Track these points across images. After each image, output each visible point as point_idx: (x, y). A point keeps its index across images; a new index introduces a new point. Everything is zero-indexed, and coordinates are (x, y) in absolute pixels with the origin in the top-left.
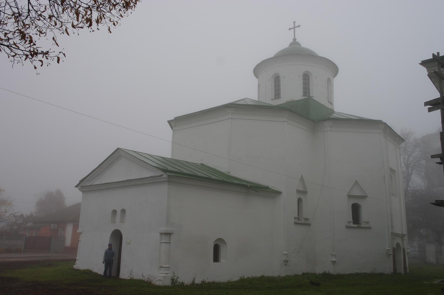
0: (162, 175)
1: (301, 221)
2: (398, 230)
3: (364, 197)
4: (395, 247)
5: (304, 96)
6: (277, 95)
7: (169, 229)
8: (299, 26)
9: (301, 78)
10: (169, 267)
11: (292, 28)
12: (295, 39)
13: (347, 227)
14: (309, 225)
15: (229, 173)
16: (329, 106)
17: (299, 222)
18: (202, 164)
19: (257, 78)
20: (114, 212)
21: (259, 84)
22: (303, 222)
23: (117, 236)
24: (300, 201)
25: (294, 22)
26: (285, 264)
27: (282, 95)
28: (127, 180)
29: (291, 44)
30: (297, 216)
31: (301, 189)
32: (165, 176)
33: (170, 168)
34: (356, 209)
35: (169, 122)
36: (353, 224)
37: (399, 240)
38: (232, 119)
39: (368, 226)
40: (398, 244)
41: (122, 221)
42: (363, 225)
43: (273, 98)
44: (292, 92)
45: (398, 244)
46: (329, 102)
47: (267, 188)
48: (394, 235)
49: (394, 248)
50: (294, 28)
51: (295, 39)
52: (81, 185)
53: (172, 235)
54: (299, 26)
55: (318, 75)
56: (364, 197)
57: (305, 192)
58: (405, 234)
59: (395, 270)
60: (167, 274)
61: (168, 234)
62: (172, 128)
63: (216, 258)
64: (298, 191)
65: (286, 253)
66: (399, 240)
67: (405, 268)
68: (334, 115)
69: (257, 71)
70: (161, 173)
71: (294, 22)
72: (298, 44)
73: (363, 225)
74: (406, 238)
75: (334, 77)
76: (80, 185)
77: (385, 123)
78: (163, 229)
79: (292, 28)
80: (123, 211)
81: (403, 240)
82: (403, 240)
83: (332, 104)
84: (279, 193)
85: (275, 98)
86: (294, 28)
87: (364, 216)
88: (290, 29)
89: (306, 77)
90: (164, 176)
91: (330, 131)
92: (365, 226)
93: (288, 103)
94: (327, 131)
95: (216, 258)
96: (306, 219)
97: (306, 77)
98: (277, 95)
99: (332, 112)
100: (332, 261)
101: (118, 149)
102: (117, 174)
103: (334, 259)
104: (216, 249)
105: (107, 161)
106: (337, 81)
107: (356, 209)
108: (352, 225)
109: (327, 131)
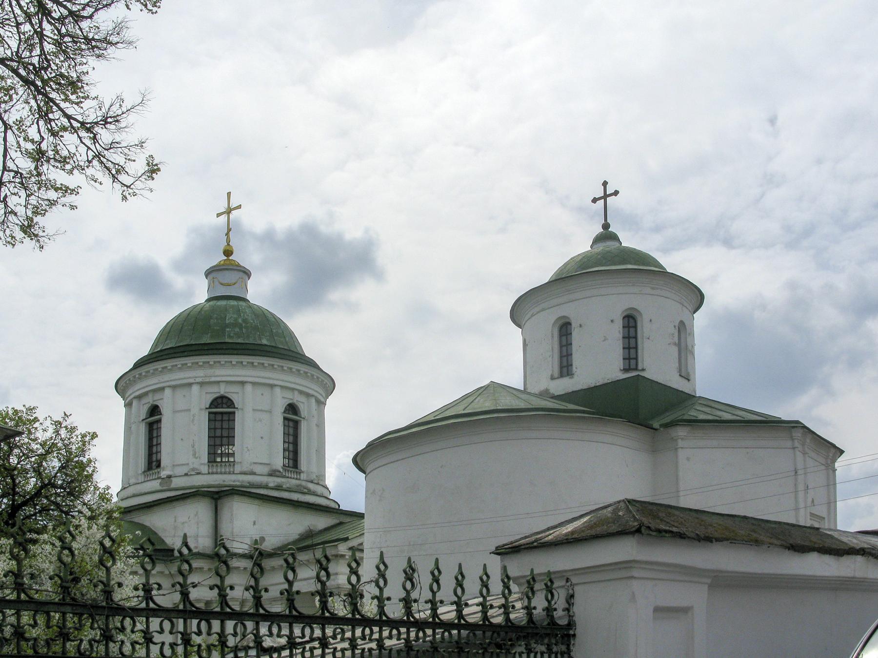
6: (565, 368)
8: (616, 193)
11: (600, 199)
12: (606, 226)
25: (605, 184)
29: (598, 240)
43: (556, 374)
50: (605, 196)
51: (606, 226)
54: (616, 193)
55: (657, 313)
69: (519, 311)
71: (605, 184)
72: (614, 237)
75: (694, 312)
79: (600, 199)
85: (561, 375)
86: (605, 196)
89: (630, 321)
97: (630, 321)
98: (565, 368)
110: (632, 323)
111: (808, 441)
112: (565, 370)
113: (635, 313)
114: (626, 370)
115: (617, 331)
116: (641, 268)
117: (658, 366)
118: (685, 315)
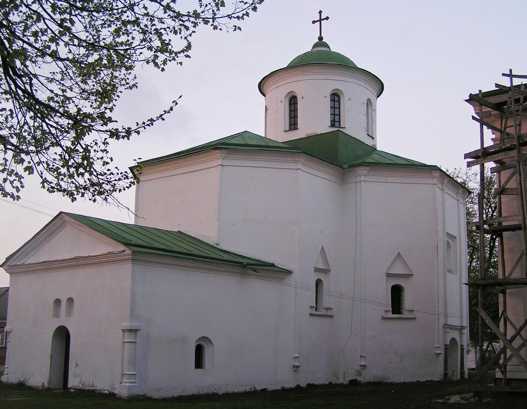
0: (124, 251)
1: (319, 311)
2: (454, 321)
3: (408, 276)
4: (448, 343)
6: (293, 125)
7: (135, 324)
8: (327, 18)
9: (329, 99)
10: (135, 374)
12: (321, 38)
13: (384, 318)
14: (331, 316)
15: (217, 244)
16: (368, 141)
17: (316, 313)
19: (264, 96)
22: (324, 312)
24: (319, 283)
25: (320, 12)
26: (295, 371)
27: (299, 125)
28: (75, 258)
29: (315, 46)
30: (314, 305)
31: (321, 266)
32: (128, 251)
33: (135, 241)
34: (397, 293)
36: (393, 313)
37: (455, 334)
38: (222, 166)
39: (412, 317)
40: (453, 340)
41: (69, 313)
42: (406, 315)
44: (314, 121)
45: (453, 340)
46: (368, 134)
47: (273, 265)
48: (447, 327)
49: (446, 345)
50: (320, 20)
51: (321, 38)
53: (138, 332)
55: (353, 92)
56: (408, 276)
57: (326, 271)
58: (464, 325)
59: (446, 375)
63: (199, 363)
65: (297, 356)
66: (455, 334)
67: (462, 373)
68: (374, 156)
70: (122, 248)
71: (320, 12)
72: (326, 45)
74: (466, 331)
75: (378, 97)
81: (461, 334)
82: (461, 334)
84: (290, 272)
85: (290, 130)
86: (320, 20)
87: (408, 302)
88: (314, 22)
90: (126, 253)
91: (365, 181)
92: (409, 317)
93: (308, 138)
94: (361, 181)
95: (199, 363)
96: (327, 309)
98: (293, 125)
99: (374, 149)
102: (61, 249)
103: (363, 363)
104: (199, 350)
106: (380, 103)
107: (397, 293)
108: (390, 315)
109: (361, 181)
110: (336, 99)
112: (292, 126)
114: (333, 125)
115: (327, 103)
116: (343, 64)
117: (353, 126)
118: (373, 97)
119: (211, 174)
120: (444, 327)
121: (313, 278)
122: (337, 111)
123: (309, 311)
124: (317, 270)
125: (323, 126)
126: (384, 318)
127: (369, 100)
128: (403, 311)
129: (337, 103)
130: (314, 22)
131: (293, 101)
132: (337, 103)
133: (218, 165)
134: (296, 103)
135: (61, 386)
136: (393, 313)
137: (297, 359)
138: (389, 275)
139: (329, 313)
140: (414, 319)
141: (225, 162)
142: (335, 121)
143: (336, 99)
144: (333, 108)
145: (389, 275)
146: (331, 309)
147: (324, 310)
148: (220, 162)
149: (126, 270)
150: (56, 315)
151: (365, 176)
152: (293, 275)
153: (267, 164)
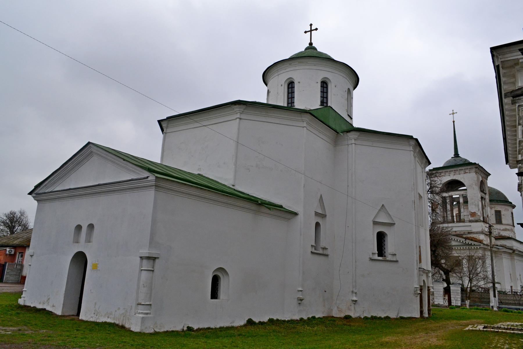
0: (148, 177)
3: (392, 224)
5: (321, 105)
7: (154, 252)
8: (316, 29)
9: (319, 85)
10: (150, 305)
12: (311, 44)
13: (372, 260)
14: (327, 255)
15: (233, 186)
16: (348, 119)
17: (315, 251)
18: (199, 174)
20: (79, 228)
21: (268, 91)
22: (321, 251)
23: (80, 259)
24: (317, 225)
25: (311, 25)
26: (299, 303)
29: (306, 49)
31: (320, 211)
32: (152, 177)
34: (381, 237)
35: (160, 122)
36: (378, 256)
38: (240, 119)
39: (395, 260)
41: (88, 240)
42: (389, 258)
47: (281, 207)
50: (311, 31)
51: (311, 44)
52: (36, 192)
53: (157, 260)
54: (316, 29)
55: (338, 83)
56: (392, 224)
60: (147, 314)
61: (152, 259)
62: (162, 130)
64: (317, 214)
65: (300, 289)
70: (146, 174)
71: (311, 25)
72: (315, 49)
73: (389, 258)
76: (36, 192)
77: (417, 140)
78: (145, 252)
80: (91, 227)
81: (427, 276)
82: (427, 276)
83: (351, 118)
84: (296, 214)
86: (311, 31)
87: (390, 247)
88: (306, 32)
89: (324, 84)
90: (149, 179)
92: (392, 259)
94: (352, 144)
96: (324, 249)
97: (324, 84)
100: (353, 301)
101: (89, 143)
104: (216, 281)
105: (73, 160)
106: (356, 93)
107: (381, 237)
108: (376, 257)
109: (352, 144)
110: (325, 86)
111: (418, 150)
113: (327, 80)
119: (230, 126)
120: (419, 271)
121: (314, 220)
122: (325, 94)
123: (310, 249)
124: (317, 214)
125: (316, 104)
126: (372, 260)
127: (349, 89)
128: (386, 254)
129: (325, 89)
130: (306, 32)
131: (291, 85)
132: (325, 89)
133: (236, 119)
134: (293, 87)
135: (75, 313)
136: (378, 256)
137: (300, 292)
138: (375, 223)
139: (325, 252)
140: (397, 261)
141: (243, 116)
142: (324, 101)
143: (325, 86)
144: (322, 92)
145: (375, 223)
146: (326, 249)
147: (321, 250)
148: (238, 116)
149: (149, 196)
150: (76, 241)
151: (355, 140)
152: (299, 216)
153: (277, 121)
